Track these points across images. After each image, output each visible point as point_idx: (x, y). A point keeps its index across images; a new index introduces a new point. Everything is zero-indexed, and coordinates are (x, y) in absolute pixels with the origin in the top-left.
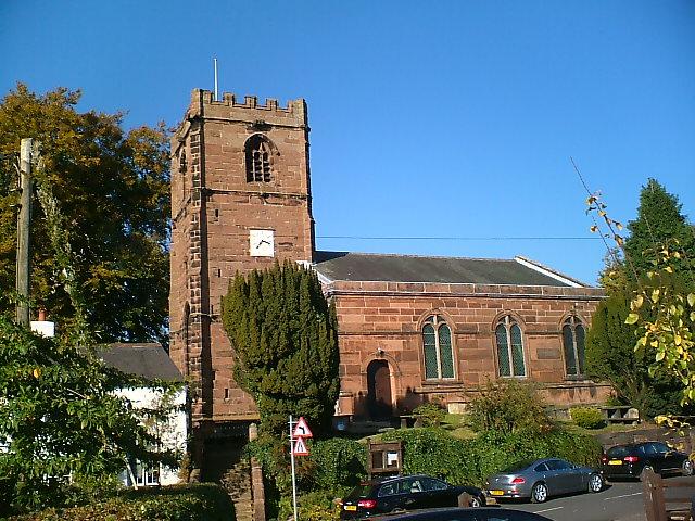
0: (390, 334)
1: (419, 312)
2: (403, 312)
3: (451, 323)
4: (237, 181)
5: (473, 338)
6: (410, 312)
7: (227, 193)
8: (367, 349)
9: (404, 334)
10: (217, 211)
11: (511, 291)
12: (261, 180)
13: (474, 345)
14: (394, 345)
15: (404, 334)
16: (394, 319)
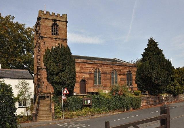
2: (90, 68)
3: (101, 71)
5: (106, 75)
6: (91, 68)
7: (47, 37)
8: (80, 77)
9: (90, 73)
10: (44, 42)
11: (115, 63)
13: (106, 77)
14: (87, 76)
15: (90, 73)
16: (87, 69)
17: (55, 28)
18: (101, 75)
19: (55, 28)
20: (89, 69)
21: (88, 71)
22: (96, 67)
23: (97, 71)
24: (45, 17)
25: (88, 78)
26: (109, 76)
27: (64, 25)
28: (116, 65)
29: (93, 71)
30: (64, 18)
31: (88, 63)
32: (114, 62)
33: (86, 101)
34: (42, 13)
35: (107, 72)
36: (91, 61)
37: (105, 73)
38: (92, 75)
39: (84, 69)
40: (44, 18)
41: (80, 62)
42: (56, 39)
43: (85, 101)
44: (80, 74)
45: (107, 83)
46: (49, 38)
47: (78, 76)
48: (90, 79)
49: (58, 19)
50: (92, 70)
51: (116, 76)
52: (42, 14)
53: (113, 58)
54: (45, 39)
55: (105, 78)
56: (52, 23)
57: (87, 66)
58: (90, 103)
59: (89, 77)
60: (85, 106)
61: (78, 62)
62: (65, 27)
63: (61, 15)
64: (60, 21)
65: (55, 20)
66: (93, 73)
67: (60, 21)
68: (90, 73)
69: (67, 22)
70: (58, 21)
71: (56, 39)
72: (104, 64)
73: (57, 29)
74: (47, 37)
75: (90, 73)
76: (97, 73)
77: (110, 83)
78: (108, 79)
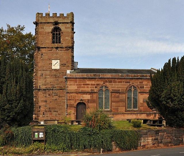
0: (86, 93)
1: (98, 85)
2: (92, 85)
3: (111, 89)
4: (49, 43)
5: (118, 94)
6: (94, 85)
7: (45, 48)
8: (77, 98)
9: (91, 93)
10: (42, 54)
11: (135, 76)
12: (57, 43)
13: (118, 97)
14: (87, 97)
15: (91, 93)
16: (88, 87)
17: (56, 33)
18: (110, 94)
19: (56, 33)
20: (91, 87)
21: (89, 90)
22: (102, 83)
23: (104, 89)
24: (44, 21)
25: (88, 100)
26: (123, 96)
27: (68, 28)
28: (134, 79)
29: (96, 90)
30: (70, 18)
31: (89, 78)
32: (133, 75)
33: (36, 134)
34: (40, 15)
35: (120, 90)
36: (94, 75)
37: (117, 92)
38: (95, 96)
39: (82, 87)
40: (42, 23)
41: (76, 78)
42: (57, 48)
43: (36, 133)
44: (76, 95)
45: (120, 106)
46: (48, 48)
47: (74, 98)
48: (92, 101)
49: (60, 21)
50: (96, 87)
51: (135, 95)
52: (40, 17)
53: (150, 69)
54: (43, 50)
55: (117, 99)
56: (53, 27)
57: (88, 82)
58: (43, 136)
59: (89, 98)
60: (35, 141)
61: (73, 78)
62: (70, 30)
63: (65, 15)
64: (63, 23)
65: (56, 23)
66: (96, 93)
67: (63, 23)
68: (91, 93)
69: (73, 23)
70: (61, 23)
71: (57, 48)
72: (115, 79)
73: (59, 34)
74: (45, 48)
75: (93, 93)
76: (104, 93)
77: (124, 106)
78: (121, 101)
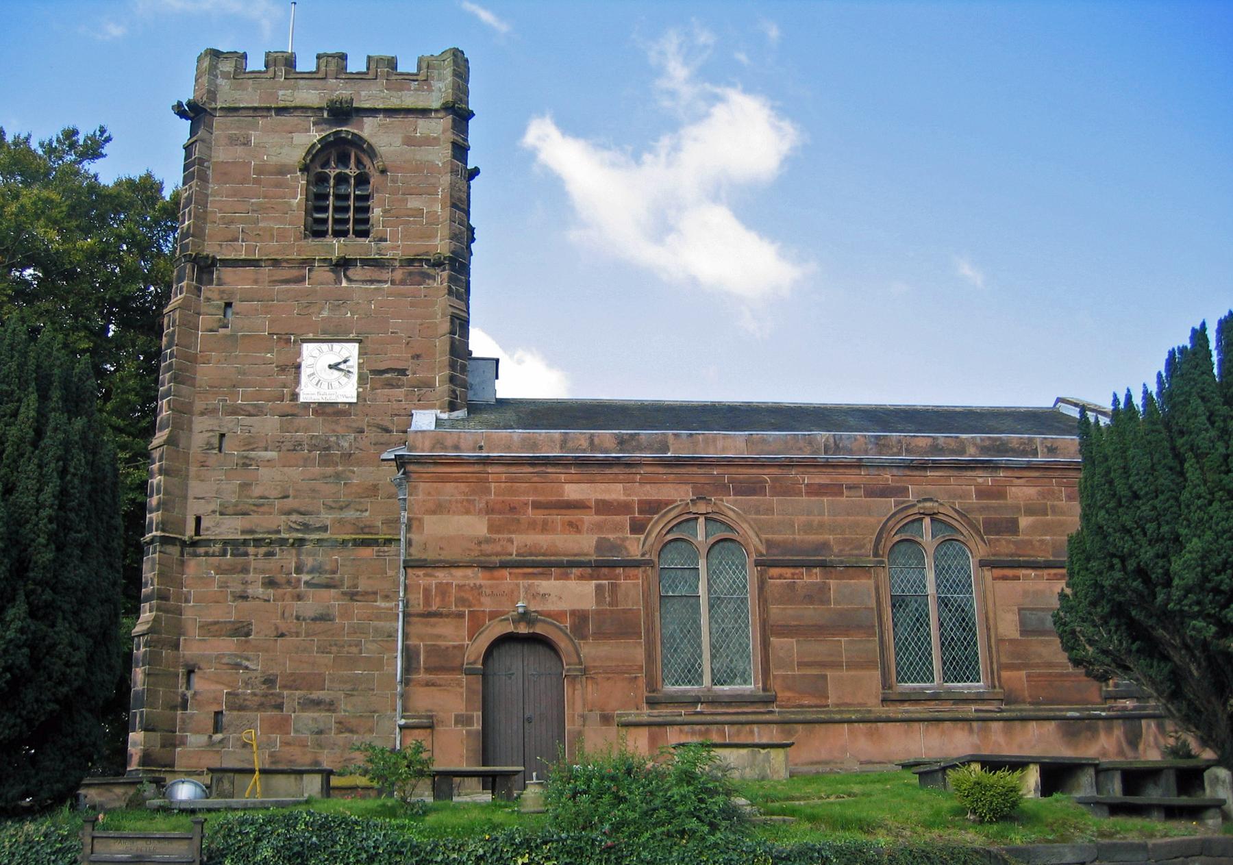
0: (559, 565)
1: (652, 507)
2: (604, 507)
4: (282, 235)
5: (813, 578)
6: (623, 508)
7: (254, 263)
8: (488, 605)
11: (935, 449)
12: (344, 234)
13: (818, 595)
16: (574, 527)
18: (752, 573)
20: (599, 527)
21: (584, 543)
22: (677, 493)
24: (249, 97)
25: (580, 618)
27: (428, 141)
28: (936, 466)
29: (635, 547)
30: (437, 85)
31: (582, 463)
32: (922, 440)
34: (227, 66)
35: (825, 546)
36: (622, 442)
38: (632, 587)
39: (532, 526)
40: (236, 109)
41: (486, 461)
44: (474, 577)
45: (836, 665)
46: (276, 263)
47: (462, 601)
49: (366, 97)
50: (637, 528)
52: (226, 75)
54: (236, 281)
55: (810, 613)
56: (315, 136)
59: (589, 604)
62: (441, 155)
63: (407, 65)
65: (341, 112)
68: (599, 565)
69: (460, 115)
70: (373, 112)
71: (343, 264)
72: (789, 464)
73: (362, 180)
74: (254, 263)
75: (613, 565)
76: (702, 565)
77: (867, 665)
78: (845, 624)
